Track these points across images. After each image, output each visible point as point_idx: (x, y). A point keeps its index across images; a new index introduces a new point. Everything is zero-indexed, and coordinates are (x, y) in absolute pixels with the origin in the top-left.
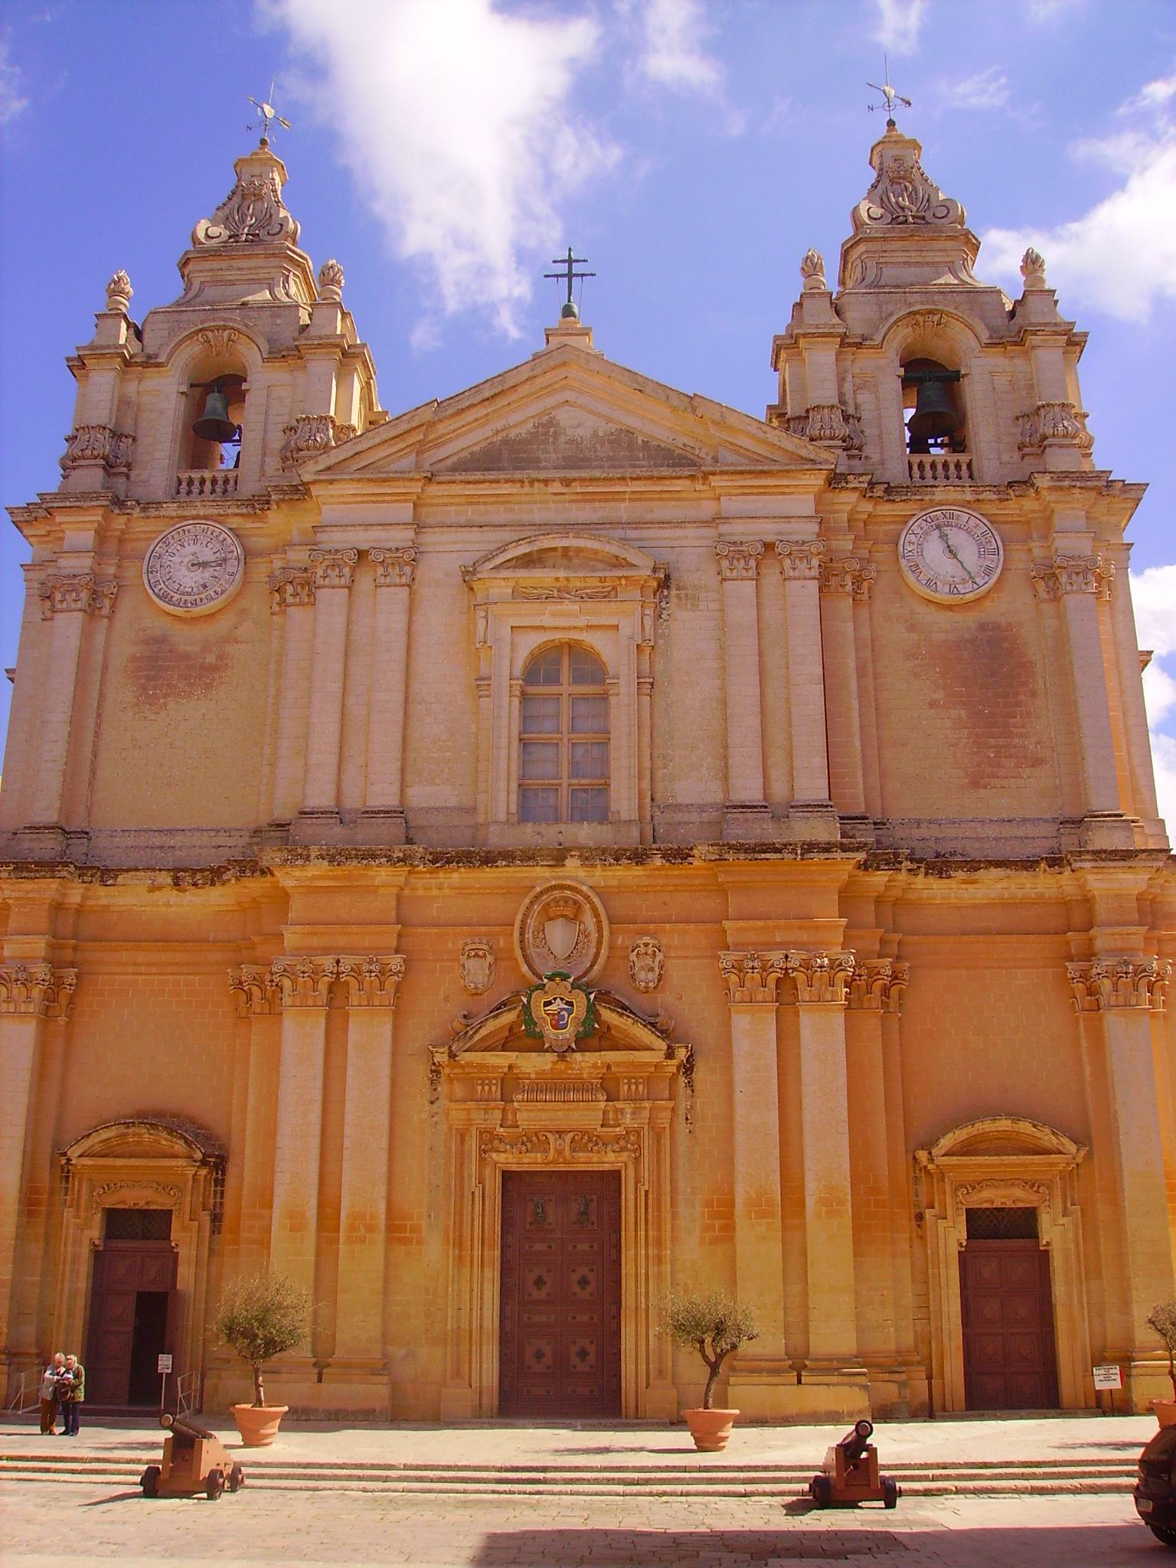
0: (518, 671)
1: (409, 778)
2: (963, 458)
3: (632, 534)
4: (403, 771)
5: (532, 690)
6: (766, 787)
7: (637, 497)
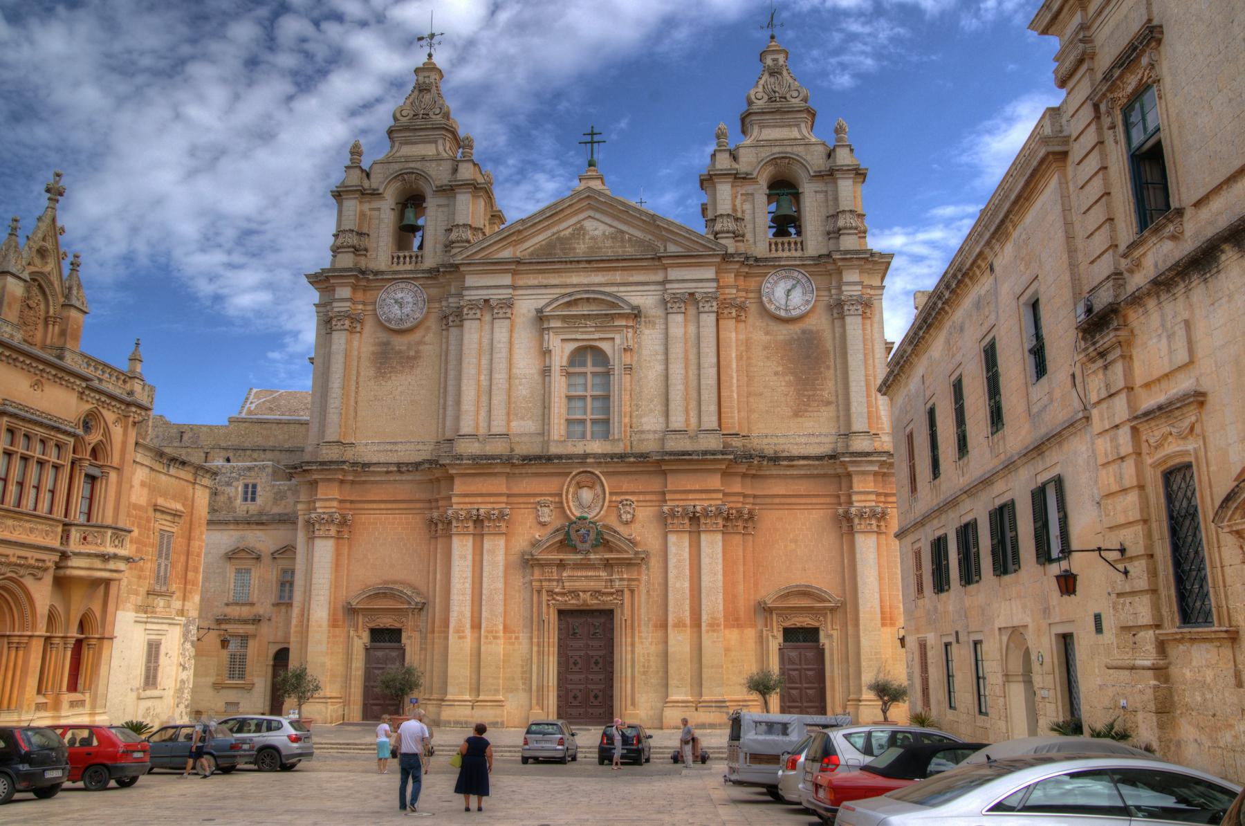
0: (564, 363)
3: (622, 289)
4: (508, 414)
5: (572, 370)
6: (687, 420)
7: (624, 269)
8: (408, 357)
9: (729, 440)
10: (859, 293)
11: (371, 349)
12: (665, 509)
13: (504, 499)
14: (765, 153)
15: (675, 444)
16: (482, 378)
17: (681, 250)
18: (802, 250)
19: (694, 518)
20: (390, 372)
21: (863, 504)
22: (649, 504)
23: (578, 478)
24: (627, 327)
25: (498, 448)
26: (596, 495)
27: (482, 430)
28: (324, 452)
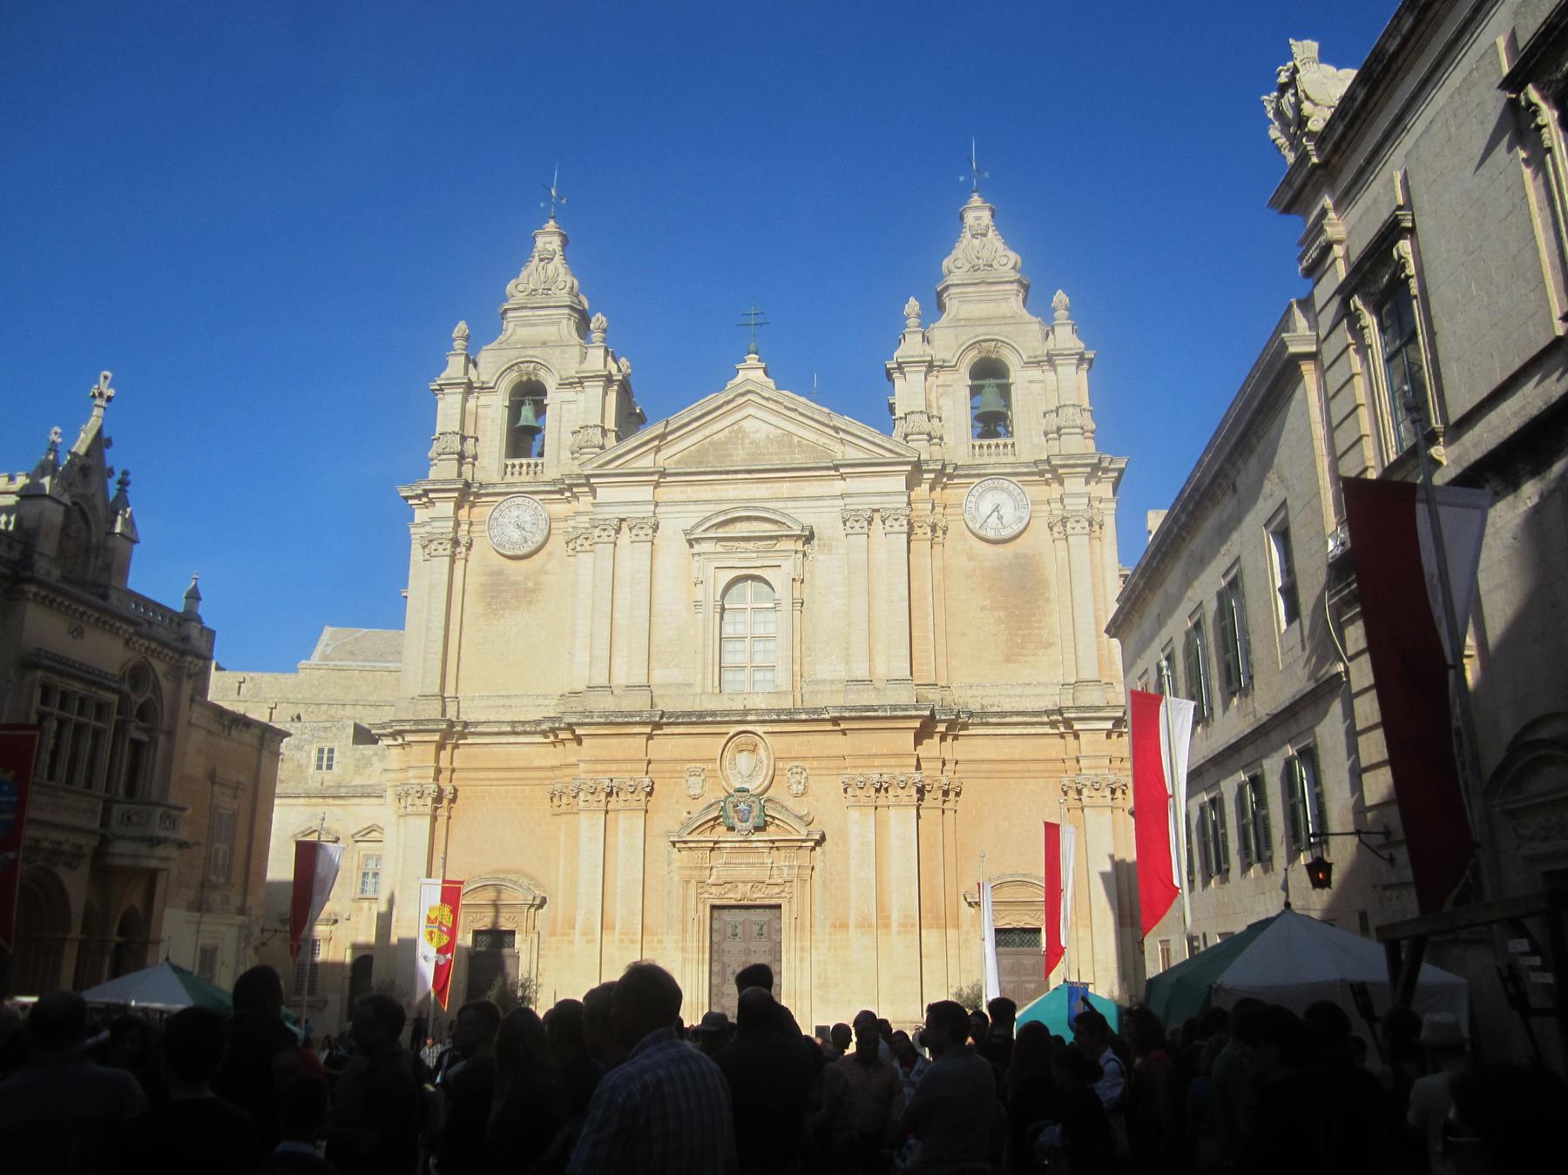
1: (653, 664)
2: (1009, 441)
9: (923, 691)
12: (845, 778)
14: (968, 337)
20: (503, 609)
22: (824, 772)
24: (796, 552)
25: (639, 702)
28: (420, 707)
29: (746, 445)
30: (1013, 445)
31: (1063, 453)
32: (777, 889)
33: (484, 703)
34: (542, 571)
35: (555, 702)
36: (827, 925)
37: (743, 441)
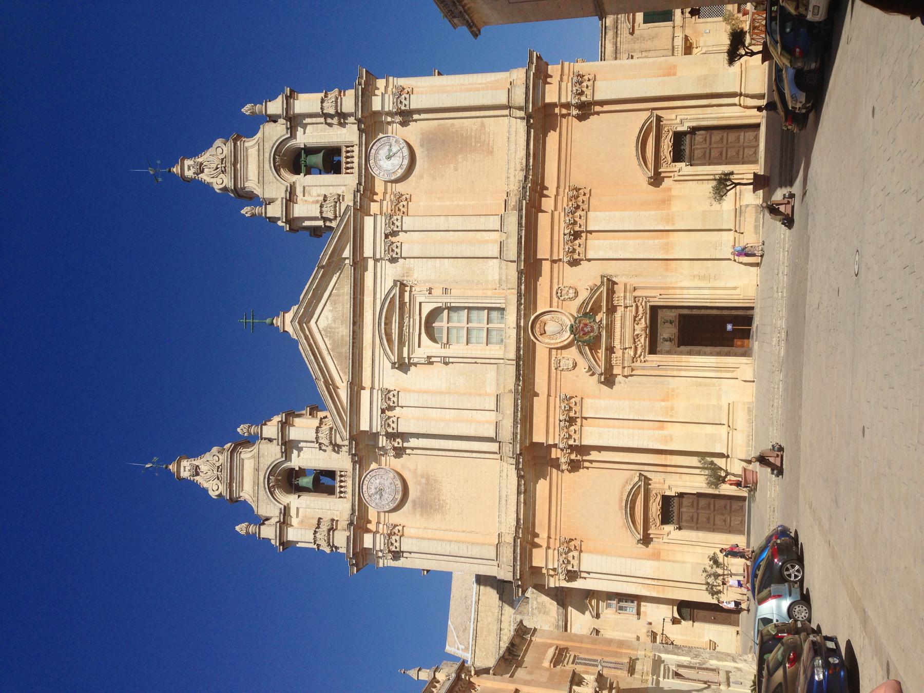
0: (439, 346)
3: (378, 296)
4: (480, 395)
8: (427, 483)
9: (510, 207)
10: (391, 96)
11: (418, 516)
13: (552, 399)
15: (512, 251)
16: (448, 417)
17: (349, 245)
18: (353, 146)
19: (576, 235)
21: (570, 93)
23: (538, 334)
24: (411, 291)
25: (508, 403)
26: (552, 319)
27: (492, 416)
28: (505, 560)
29: (336, 326)
30: (347, 147)
31: (354, 111)
32: (640, 309)
33: (503, 515)
34: (415, 473)
35: (505, 464)
36: (666, 274)
37: (334, 328)
